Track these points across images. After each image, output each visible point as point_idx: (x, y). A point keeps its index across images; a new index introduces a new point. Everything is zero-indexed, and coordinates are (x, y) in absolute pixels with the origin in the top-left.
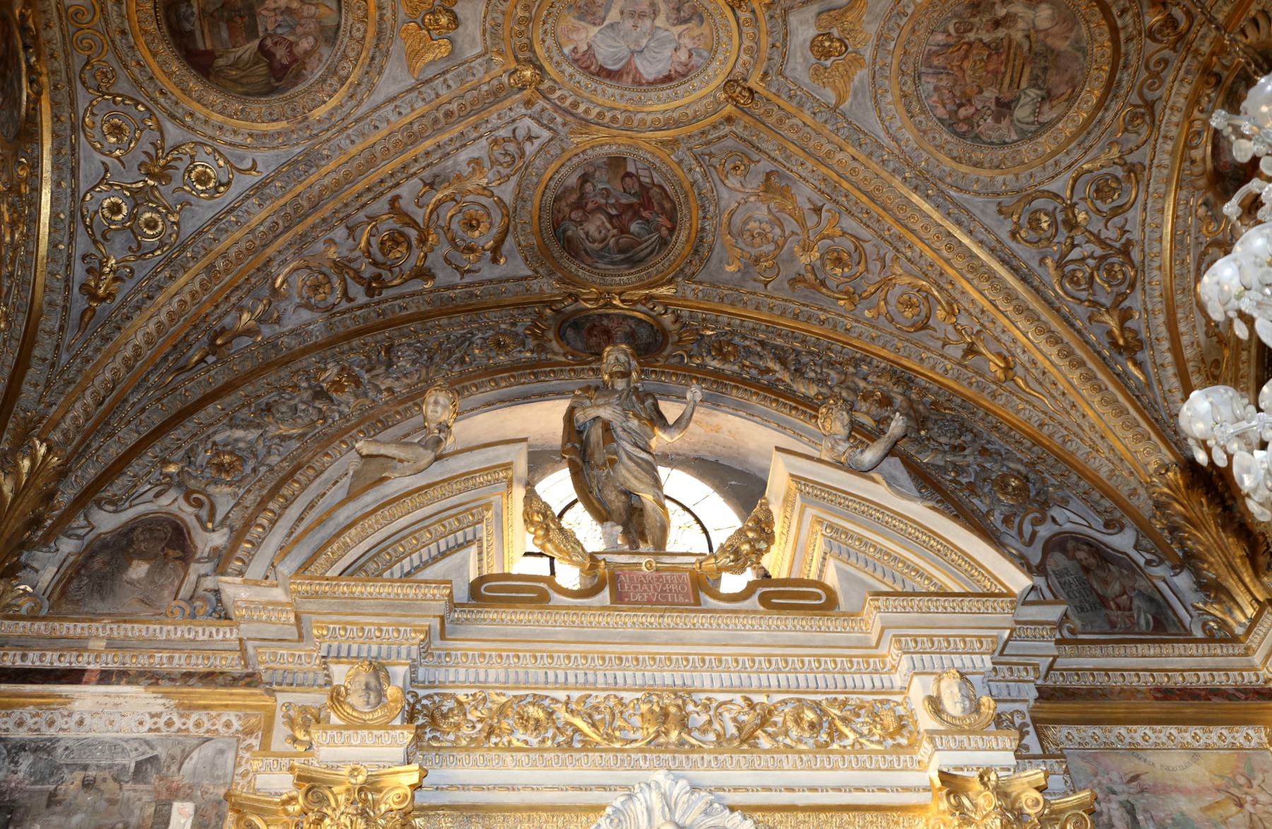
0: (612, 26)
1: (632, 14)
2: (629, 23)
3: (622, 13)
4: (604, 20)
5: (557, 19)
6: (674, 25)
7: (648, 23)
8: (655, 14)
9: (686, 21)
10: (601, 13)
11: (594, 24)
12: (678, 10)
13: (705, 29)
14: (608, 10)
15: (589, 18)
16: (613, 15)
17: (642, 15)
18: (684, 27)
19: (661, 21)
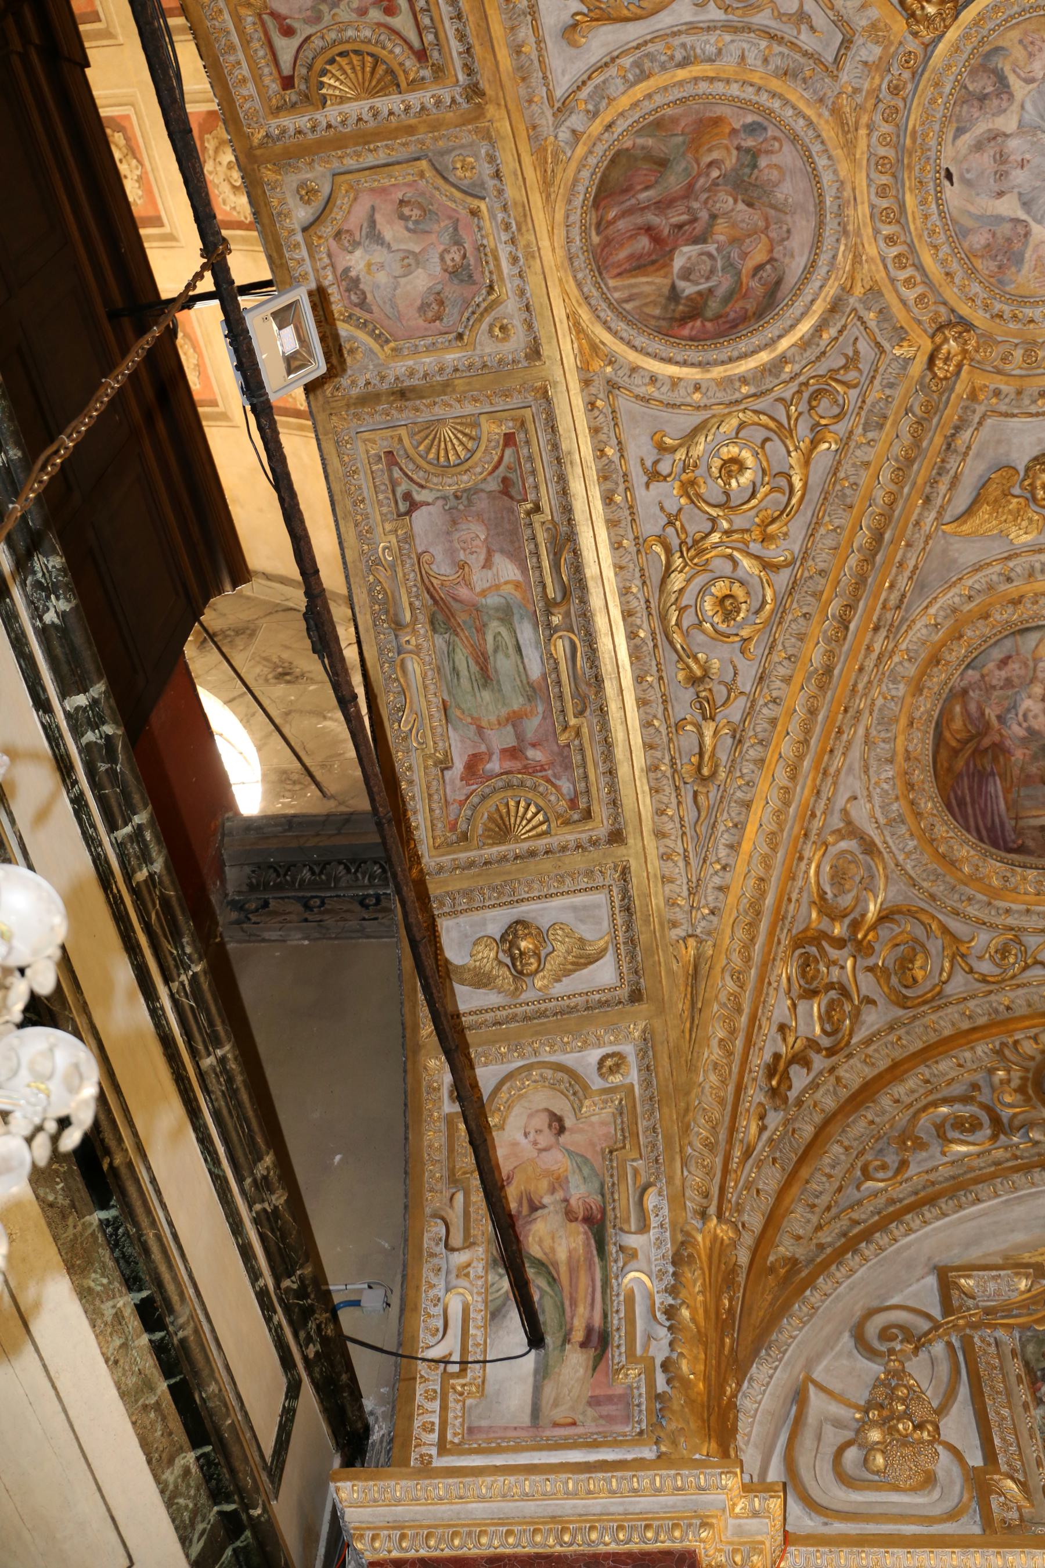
0: (1026, 205)
1: (1001, 175)
2: (1019, 177)
3: (1000, 194)
4: (1016, 221)
5: (1023, 300)
6: (1011, 96)
7: (1013, 144)
8: (995, 136)
9: (1001, 80)
10: (1006, 228)
11: (1027, 235)
12: (983, 98)
13: (1011, 39)
14: (999, 219)
15: (1017, 246)
16: (1008, 207)
17: (1002, 158)
18: (1012, 79)
19: (1008, 123)
